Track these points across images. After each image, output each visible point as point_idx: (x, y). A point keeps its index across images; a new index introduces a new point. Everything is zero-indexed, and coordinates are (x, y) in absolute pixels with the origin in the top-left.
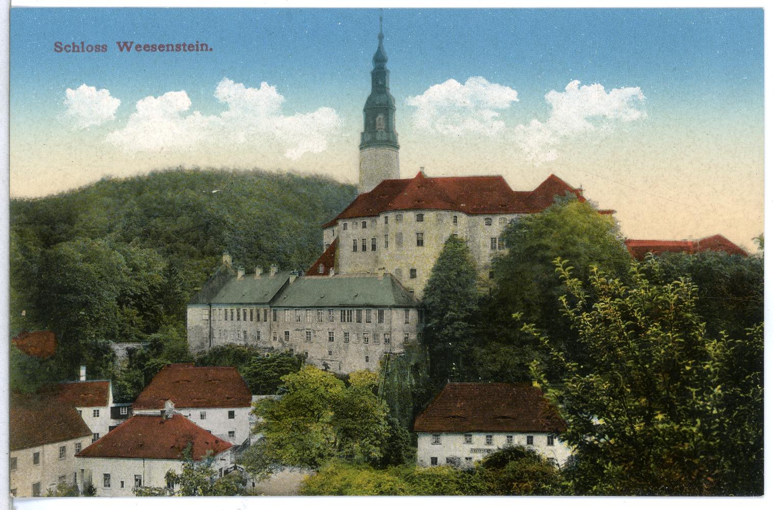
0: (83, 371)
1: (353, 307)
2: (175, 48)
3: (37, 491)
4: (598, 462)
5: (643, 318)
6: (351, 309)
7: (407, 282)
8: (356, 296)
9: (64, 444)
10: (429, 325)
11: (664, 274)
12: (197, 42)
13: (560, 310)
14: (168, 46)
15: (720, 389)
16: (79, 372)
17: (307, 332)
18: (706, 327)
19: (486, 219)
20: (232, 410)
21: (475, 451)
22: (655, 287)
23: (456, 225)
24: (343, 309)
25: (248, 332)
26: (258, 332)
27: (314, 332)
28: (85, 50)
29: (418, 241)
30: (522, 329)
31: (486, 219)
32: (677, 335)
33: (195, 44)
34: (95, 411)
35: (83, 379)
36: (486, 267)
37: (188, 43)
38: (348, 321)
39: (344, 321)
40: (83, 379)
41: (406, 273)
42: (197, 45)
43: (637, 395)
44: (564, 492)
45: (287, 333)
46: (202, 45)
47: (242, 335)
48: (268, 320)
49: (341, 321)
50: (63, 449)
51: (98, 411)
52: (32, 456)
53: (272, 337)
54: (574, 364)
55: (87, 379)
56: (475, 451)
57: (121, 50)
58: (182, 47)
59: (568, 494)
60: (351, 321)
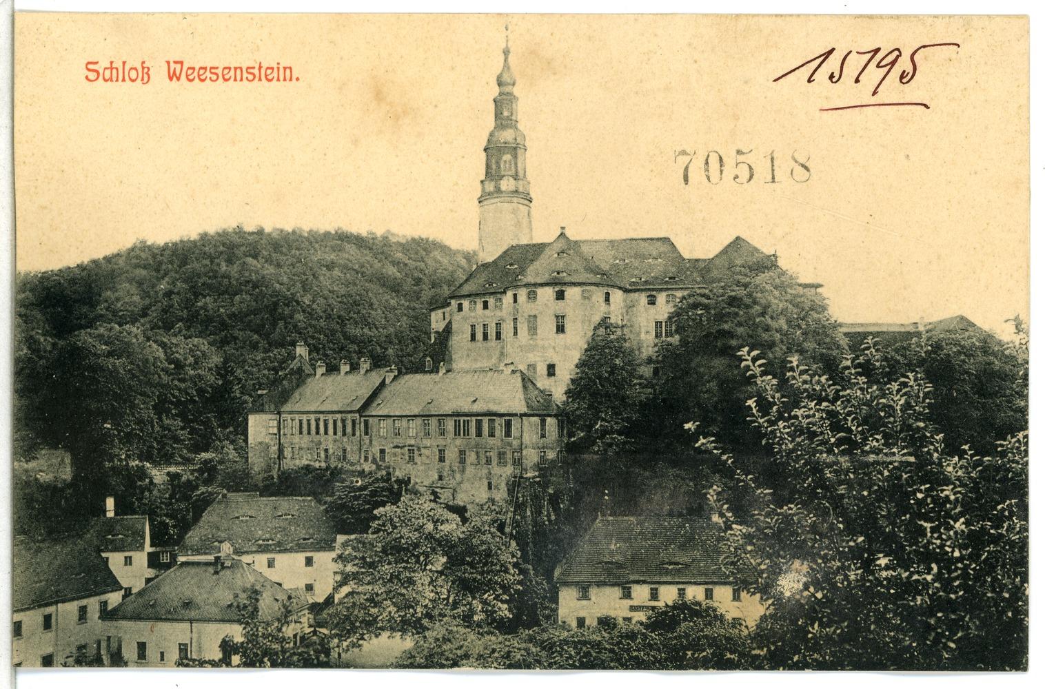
0: (110, 503)
1: (472, 415)
2: (245, 75)
3: (47, 661)
4: (800, 623)
5: (860, 429)
6: (469, 418)
7: (543, 382)
8: (475, 401)
9: (84, 602)
10: (572, 439)
11: (887, 369)
12: (278, 64)
13: (748, 419)
14: (236, 69)
15: (963, 523)
16: (105, 505)
17: (409, 450)
18: (944, 440)
19: (648, 297)
20: (309, 554)
21: (633, 608)
22: (875, 387)
23: (609, 304)
24: (457, 418)
25: (331, 451)
26: (345, 451)
27: (419, 449)
28: (127, 78)
29: (558, 326)
30: (697, 445)
31: (648, 297)
32: (905, 451)
33: (275, 66)
34: (126, 558)
35: (110, 514)
36: (649, 361)
37: (265, 65)
38: (464, 435)
39: (459, 435)
40: (110, 514)
41: (542, 369)
42: (278, 68)
43: (851, 530)
44: (755, 664)
45: (382, 451)
46: (285, 68)
47: (323, 455)
48: (358, 433)
49: (455, 435)
50: (83, 611)
51: (130, 557)
52: (41, 620)
53: (363, 458)
54: (767, 491)
55: (116, 514)
56: (633, 608)
57: (171, 79)
58: (256, 71)
59: (759, 668)
60: (468, 435)
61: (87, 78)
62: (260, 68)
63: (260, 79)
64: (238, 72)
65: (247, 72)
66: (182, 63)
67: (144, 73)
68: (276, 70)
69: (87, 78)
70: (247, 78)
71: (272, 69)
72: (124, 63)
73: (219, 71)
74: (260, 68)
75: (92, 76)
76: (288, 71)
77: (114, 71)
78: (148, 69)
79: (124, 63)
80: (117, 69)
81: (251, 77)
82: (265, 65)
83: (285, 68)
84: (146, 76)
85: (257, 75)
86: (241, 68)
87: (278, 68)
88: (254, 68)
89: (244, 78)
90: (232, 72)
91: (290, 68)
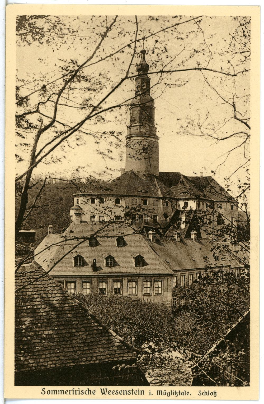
2: (127, 392)
14: (124, 391)
33: (138, 390)
57: (103, 394)
58: (131, 392)
61: (42, 393)
62: (132, 391)
63: (132, 394)
64: (125, 392)
66: (107, 389)
68: (138, 392)
69: (42, 393)
71: (137, 391)
73: (118, 392)
74: (132, 391)
75: (43, 393)
76: (142, 392)
79: (185, 391)
82: (134, 390)
83: (141, 391)
85: (131, 393)
86: (126, 391)
90: (123, 392)
91: (143, 391)
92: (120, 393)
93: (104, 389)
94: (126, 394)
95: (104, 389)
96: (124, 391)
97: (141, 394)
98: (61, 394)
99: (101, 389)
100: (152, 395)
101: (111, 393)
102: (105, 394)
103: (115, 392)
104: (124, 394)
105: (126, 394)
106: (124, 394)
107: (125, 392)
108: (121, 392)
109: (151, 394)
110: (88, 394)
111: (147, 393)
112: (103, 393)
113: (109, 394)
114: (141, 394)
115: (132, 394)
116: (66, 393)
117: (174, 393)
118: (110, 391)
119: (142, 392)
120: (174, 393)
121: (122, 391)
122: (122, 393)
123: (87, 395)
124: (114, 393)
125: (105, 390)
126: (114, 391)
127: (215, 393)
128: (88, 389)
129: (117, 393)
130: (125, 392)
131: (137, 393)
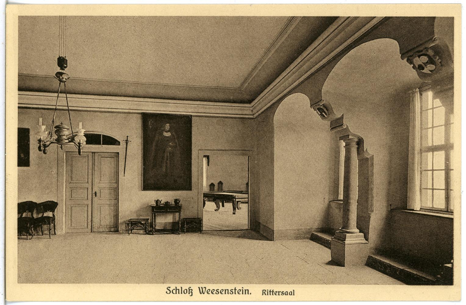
2: (229, 292)
14: (225, 290)
33: (241, 289)
42: (243, 290)
57: (201, 293)
58: (234, 291)
61: (167, 292)
62: (235, 289)
63: (235, 294)
64: (227, 291)
65: (231, 291)
67: (190, 291)
68: (242, 291)
69: (167, 292)
70: (230, 293)
71: (240, 290)
72: (181, 288)
73: (219, 291)
74: (235, 289)
75: (168, 292)
76: (247, 291)
77: (177, 291)
78: (192, 290)
79: (181, 288)
80: (179, 290)
81: (231, 293)
82: (237, 289)
83: (245, 290)
84: (191, 293)
86: (228, 290)
87: (243, 290)
88: (232, 290)
89: (229, 293)
90: (224, 291)
91: (248, 290)
92: (221, 293)
93: (202, 288)
94: (228, 293)
95: (202, 288)
96: (225, 290)
97: (245, 294)
98: (182, 293)
99: (199, 288)
100: (251, 294)
101: (210, 292)
102: (204, 293)
103: (215, 291)
104: (225, 293)
105: (228, 293)
106: (225, 293)
107: (226, 291)
108: (222, 291)
109: (249, 293)
110: (176, 293)
111: (196, 291)
112: (202, 292)
113: (208, 293)
114: (245, 294)
115: (235, 294)
116: (238, 293)
117: (269, 293)
118: (210, 290)
119: (247, 291)
120: (269, 293)
121: (223, 290)
122: (224, 292)
123: (277, 296)
124: (214, 293)
125: (204, 289)
126: (214, 290)
127: (247, 292)
128: (176, 287)
129: (217, 293)
130: (227, 291)
131: (241, 292)
